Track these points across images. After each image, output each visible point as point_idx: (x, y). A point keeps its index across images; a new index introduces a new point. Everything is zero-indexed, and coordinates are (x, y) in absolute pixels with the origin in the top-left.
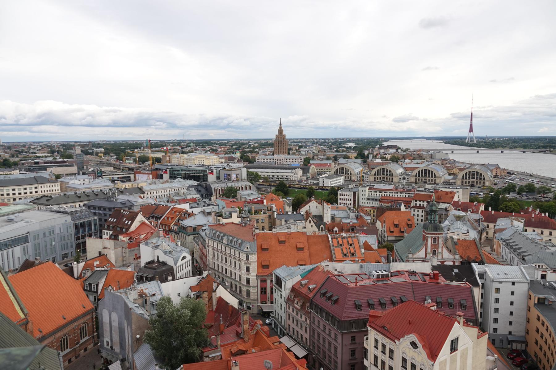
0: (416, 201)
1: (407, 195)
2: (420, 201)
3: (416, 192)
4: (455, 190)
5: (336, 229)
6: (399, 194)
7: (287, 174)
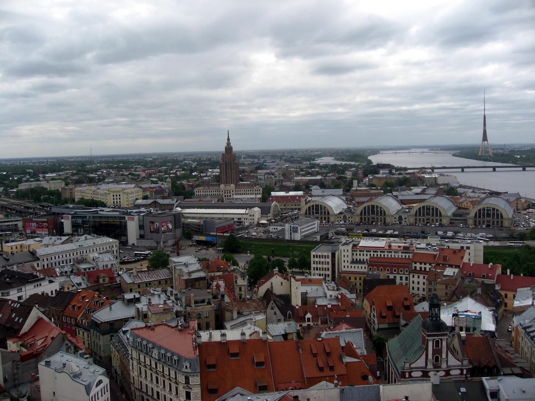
0: (415, 263)
1: (404, 255)
2: (421, 264)
3: (415, 251)
4: (465, 246)
5: (309, 315)
6: (393, 254)
7: (240, 216)
